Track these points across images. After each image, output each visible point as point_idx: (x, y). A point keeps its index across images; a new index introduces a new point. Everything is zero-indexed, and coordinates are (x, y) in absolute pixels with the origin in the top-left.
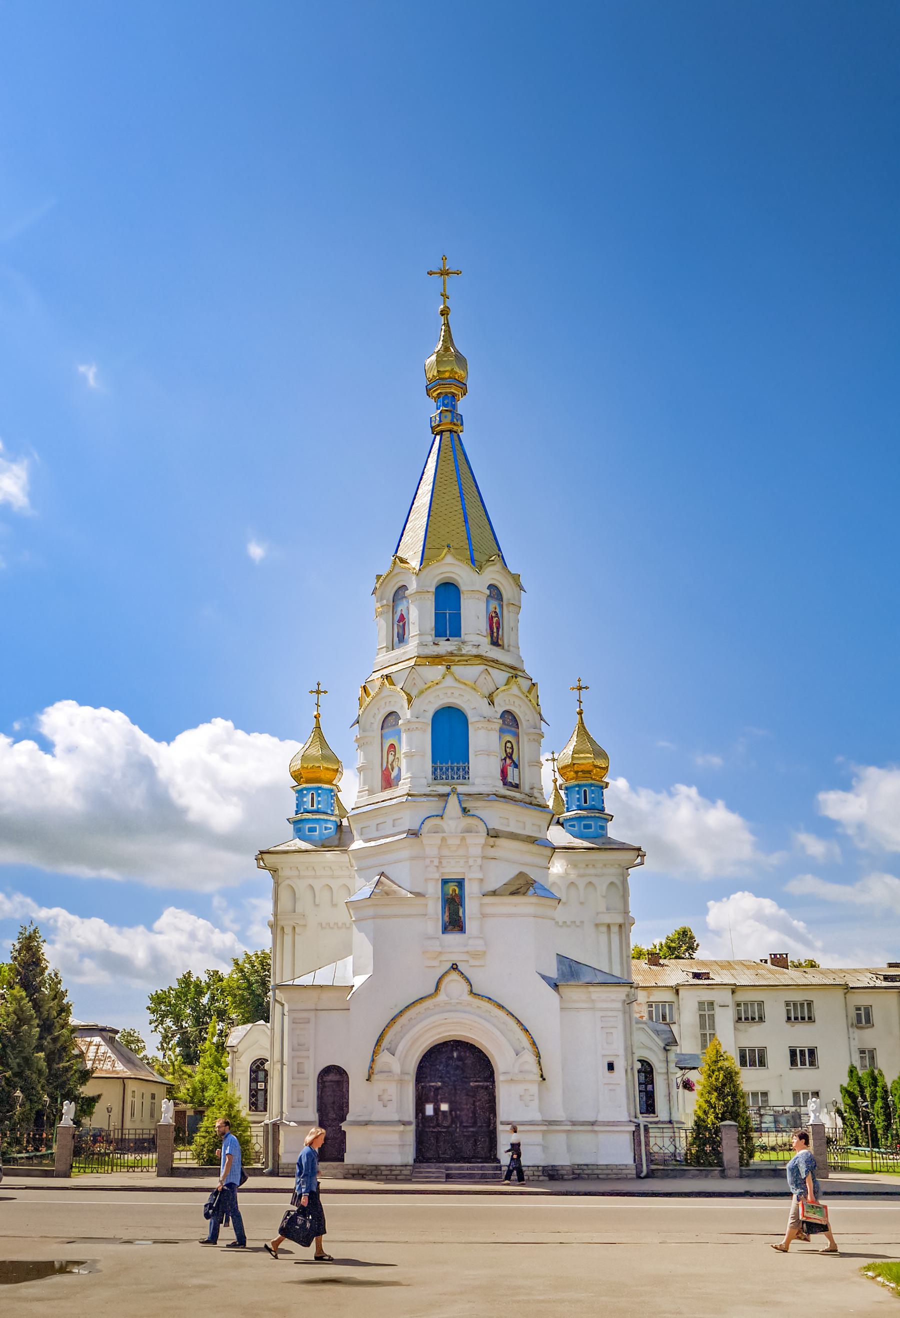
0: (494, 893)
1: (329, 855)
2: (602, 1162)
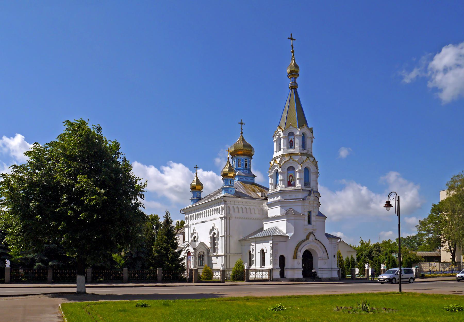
1: (239, 199)
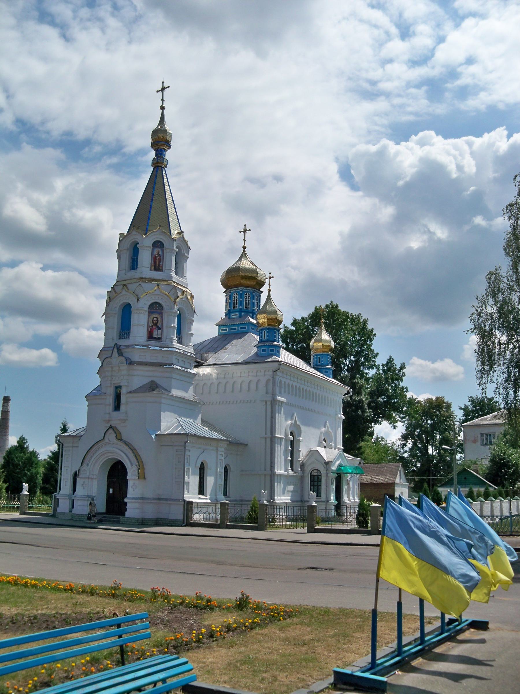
0: (134, 392)
2: (170, 518)
